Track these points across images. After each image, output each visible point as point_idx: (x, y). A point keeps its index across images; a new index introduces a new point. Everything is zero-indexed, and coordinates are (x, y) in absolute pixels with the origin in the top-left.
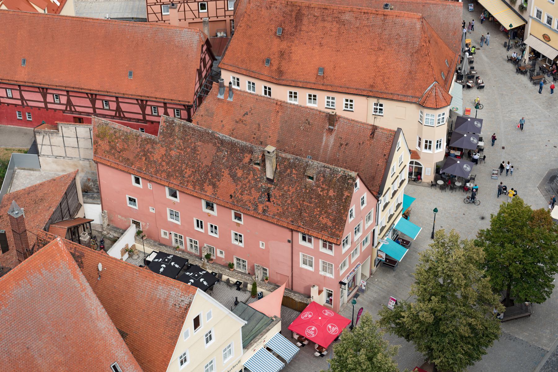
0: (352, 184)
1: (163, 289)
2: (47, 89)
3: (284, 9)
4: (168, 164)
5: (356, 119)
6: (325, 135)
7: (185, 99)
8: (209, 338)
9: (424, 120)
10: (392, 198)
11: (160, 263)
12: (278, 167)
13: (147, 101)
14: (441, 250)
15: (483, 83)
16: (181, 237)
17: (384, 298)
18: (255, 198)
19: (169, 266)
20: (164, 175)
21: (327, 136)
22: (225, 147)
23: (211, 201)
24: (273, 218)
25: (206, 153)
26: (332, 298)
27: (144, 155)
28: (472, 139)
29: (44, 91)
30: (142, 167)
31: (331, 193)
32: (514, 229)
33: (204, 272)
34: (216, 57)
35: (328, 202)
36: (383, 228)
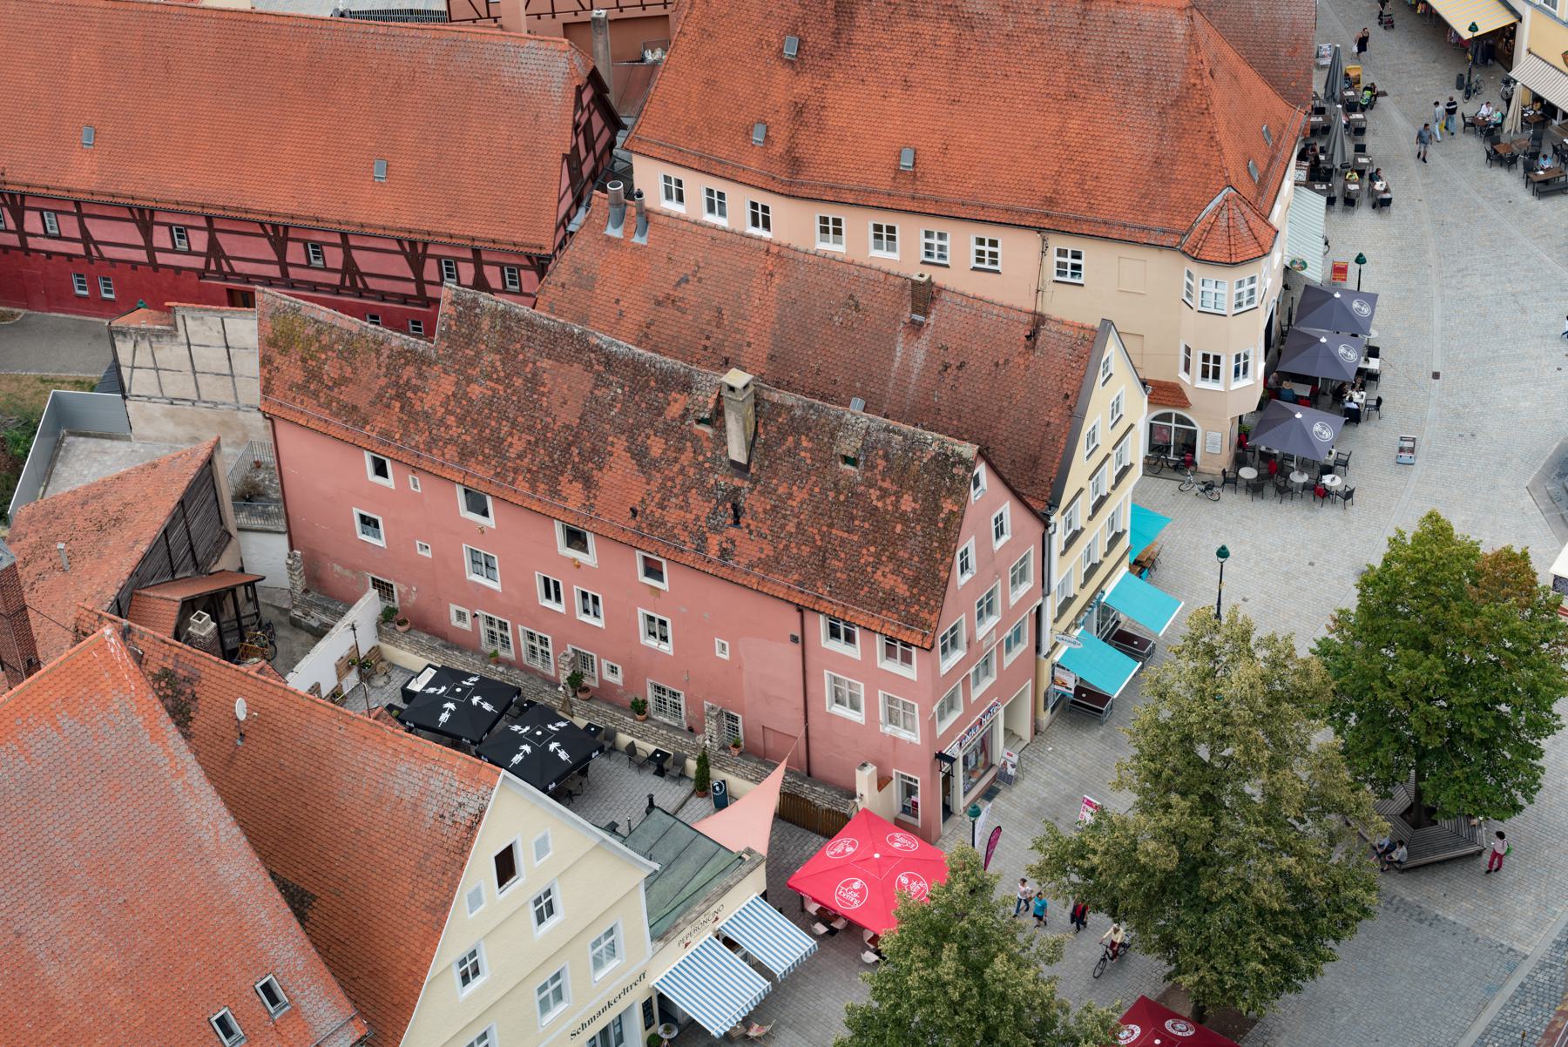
0: (963, 479)
1: (409, 771)
2: (152, 211)
4: (461, 421)
5: (988, 296)
8: (545, 909)
9: (1197, 295)
10: (1090, 518)
11: (442, 699)
12: (761, 430)
13: (426, 244)
14: (1204, 664)
15: (1386, 191)
16: (503, 626)
17: (1070, 799)
18: (697, 518)
19: (464, 708)
20: (451, 452)
23: (580, 526)
24: (747, 574)
25: (566, 390)
26: (918, 798)
28: (1342, 350)
29: (144, 218)
30: (393, 429)
31: (907, 504)
32: (1434, 607)
33: (563, 724)
35: (899, 528)
36: (1068, 602)
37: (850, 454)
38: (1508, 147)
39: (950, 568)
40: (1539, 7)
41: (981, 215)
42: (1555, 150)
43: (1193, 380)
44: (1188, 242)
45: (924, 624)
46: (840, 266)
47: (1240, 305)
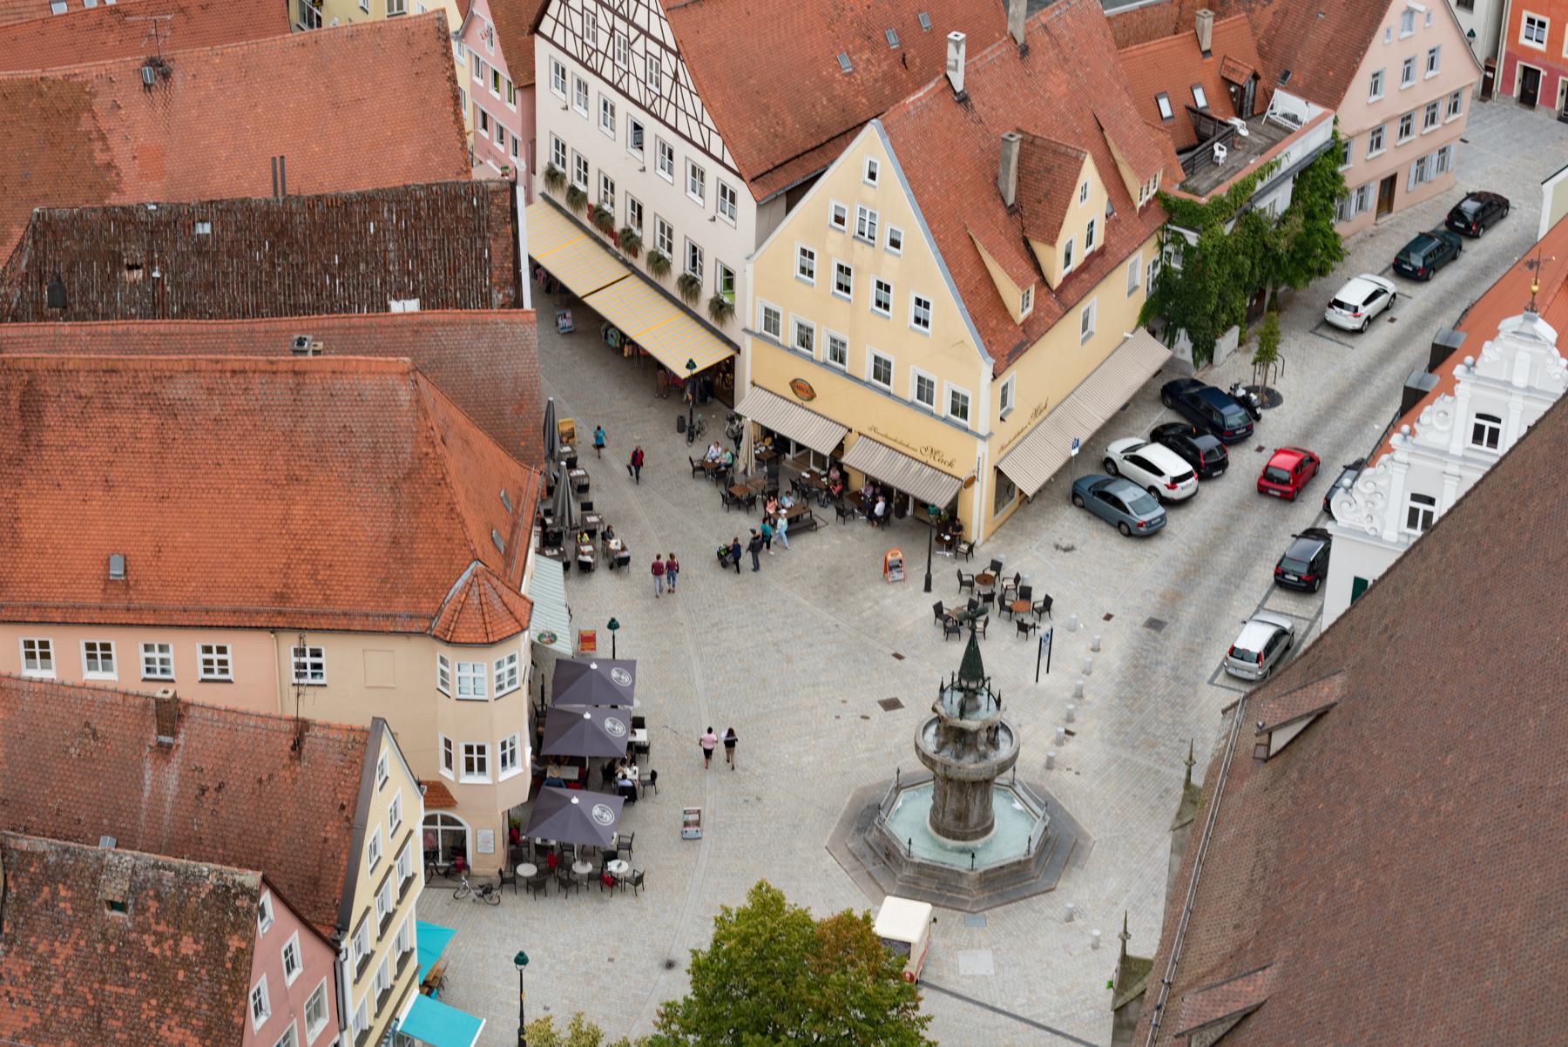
0: (249, 912)
5: (242, 707)
6: (148, 765)
10: (379, 939)
12: (11, 884)
15: (623, 549)
31: (188, 946)
35: (181, 975)
37: (118, 899)
38: (744, 488)
40: (760, 336)
41: (207, 621)
42: (794, 485)
43: (457, 776)
44: (438, 625)
46: (71, 692)
47: (501, 687)
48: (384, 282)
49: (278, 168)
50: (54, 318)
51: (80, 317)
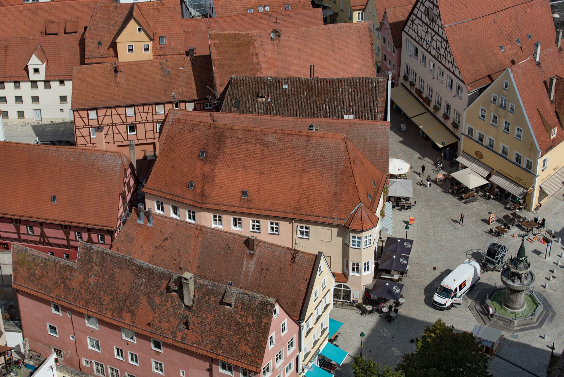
3: (207, 132)
4: (86, 291)
6: (245, 260)
7: (109, 224)
10: (315, 324)
12: (196, 294)
16: (102, 366)
20: (82, 302)
21: (248, 261)
22: (142, 274)
27: (63, 282)
31: (250, 320)
34: (141, 181)
39: (266, 343)
45: (257, 364)
48: (343, 108)
49: (312, 68)
50: (235, 112)
51: (244, 112)
